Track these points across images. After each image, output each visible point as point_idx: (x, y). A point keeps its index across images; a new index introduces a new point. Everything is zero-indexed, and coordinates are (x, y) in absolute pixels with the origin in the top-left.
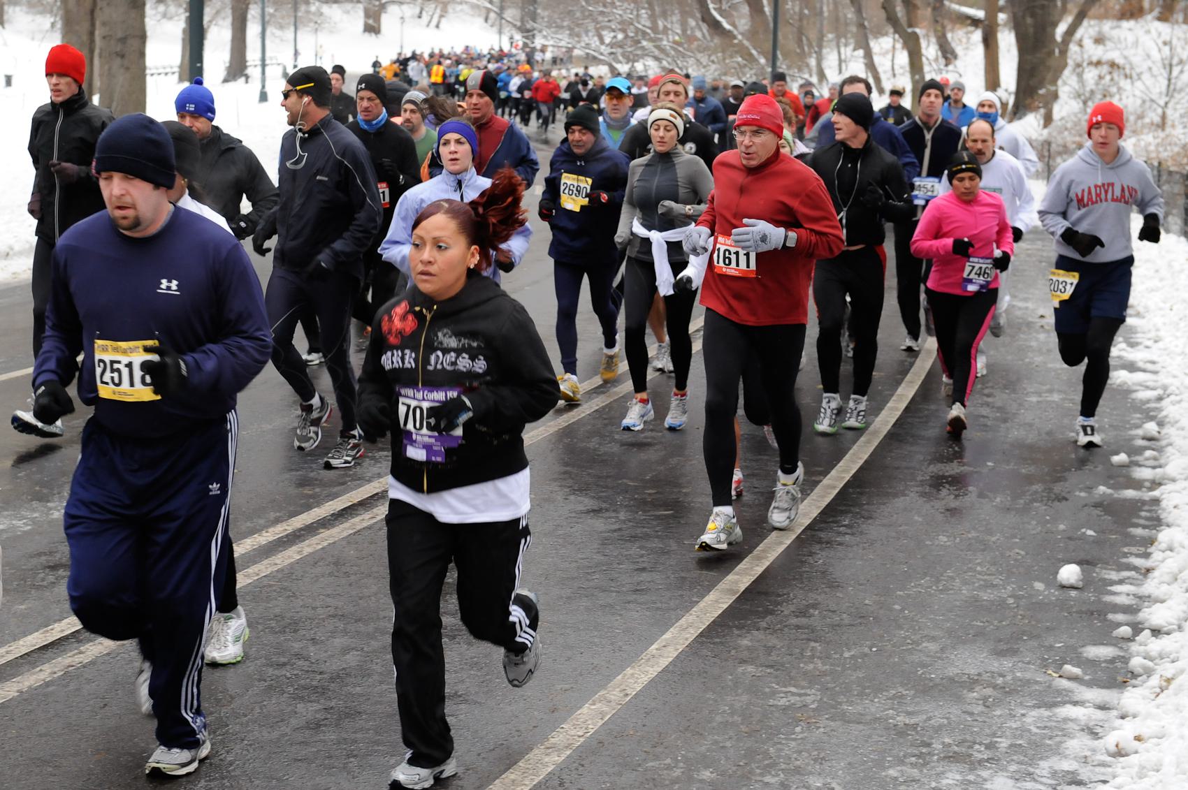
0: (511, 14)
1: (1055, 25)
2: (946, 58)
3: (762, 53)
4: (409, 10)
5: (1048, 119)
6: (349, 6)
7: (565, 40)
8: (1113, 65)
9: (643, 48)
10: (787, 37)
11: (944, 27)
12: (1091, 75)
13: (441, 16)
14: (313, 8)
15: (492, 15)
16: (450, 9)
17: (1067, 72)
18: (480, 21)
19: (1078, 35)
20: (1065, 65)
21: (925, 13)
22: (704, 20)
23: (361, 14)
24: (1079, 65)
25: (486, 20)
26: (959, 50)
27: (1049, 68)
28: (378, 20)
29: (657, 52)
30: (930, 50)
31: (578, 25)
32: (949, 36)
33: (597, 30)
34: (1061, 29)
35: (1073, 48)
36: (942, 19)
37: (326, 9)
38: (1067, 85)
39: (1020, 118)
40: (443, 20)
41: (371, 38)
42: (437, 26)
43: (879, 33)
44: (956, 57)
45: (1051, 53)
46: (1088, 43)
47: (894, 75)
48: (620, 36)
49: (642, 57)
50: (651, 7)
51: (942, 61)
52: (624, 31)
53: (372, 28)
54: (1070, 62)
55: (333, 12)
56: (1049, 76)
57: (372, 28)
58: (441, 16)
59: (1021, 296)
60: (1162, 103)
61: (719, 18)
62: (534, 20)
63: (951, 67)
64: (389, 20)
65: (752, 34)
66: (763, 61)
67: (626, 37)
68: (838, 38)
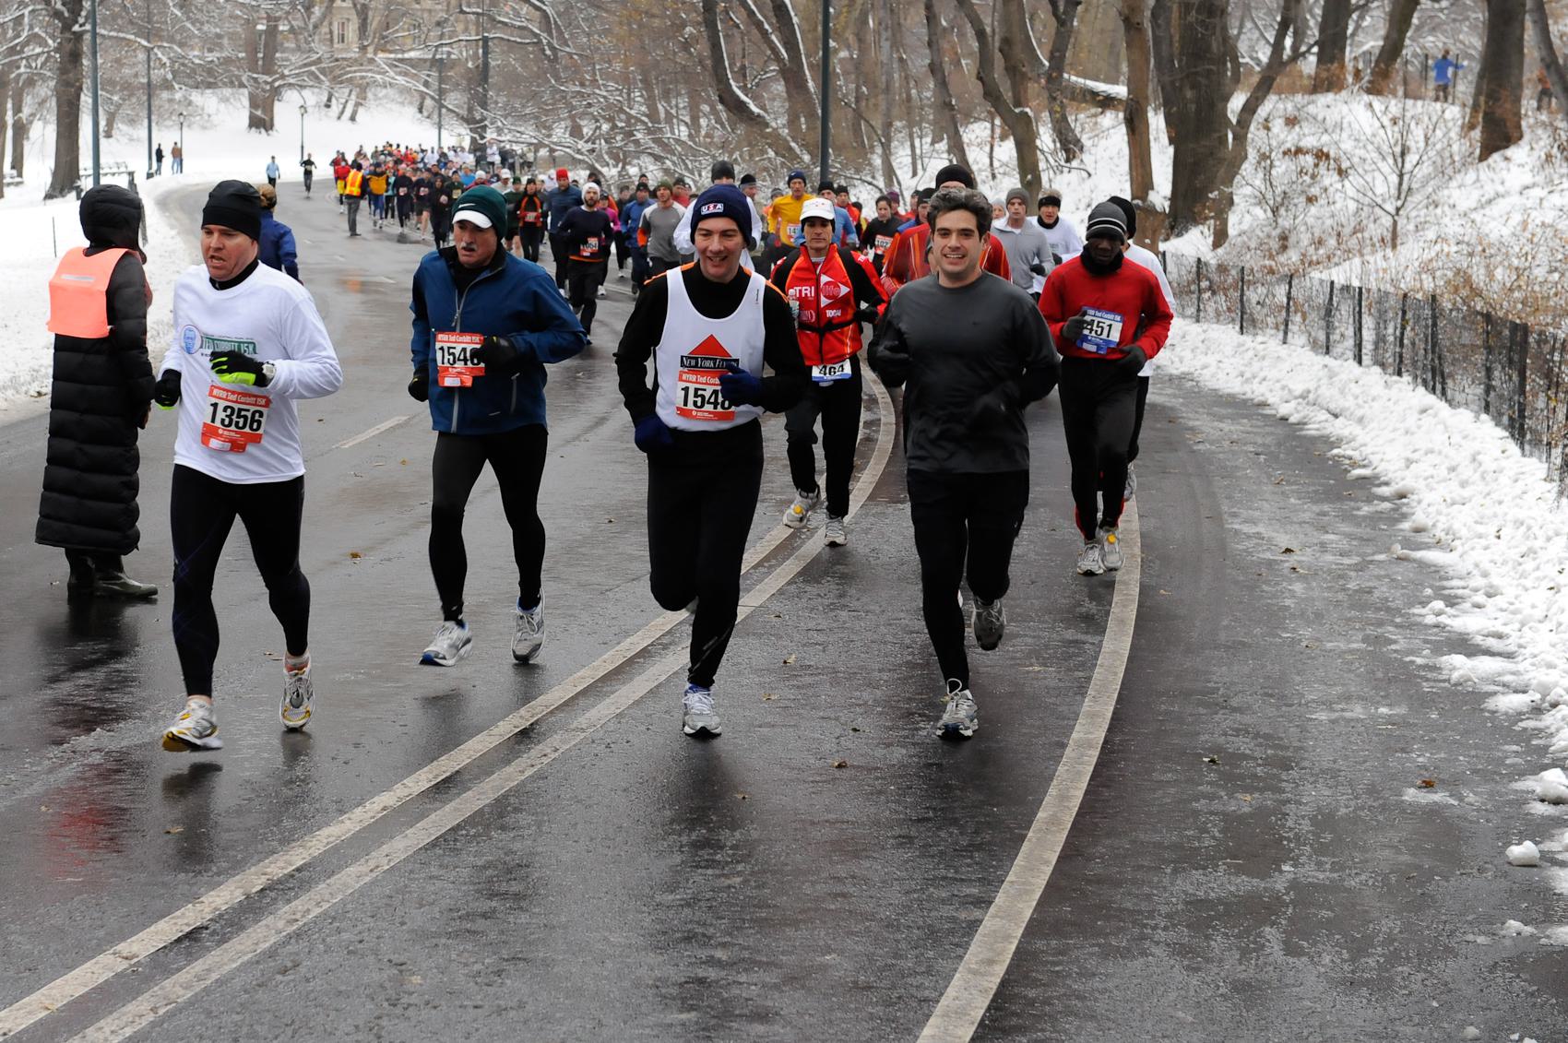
0: (455, 99)
1: (1227, 99)
2: (1067, 151)
3: (804, 146)
4: (312, 97)
5: (1220, 237)
6: (227, 92)
7: (529, 133)
8: (1321, 155)
9: (637, 142)
10: (840, 127)
11: (1062, 106)
12: (1282, 168)
13: (358, 105)
14: (178, 96)
15: (428, 102)
16: (370, 95)
17: (1247, 168)
18: (411, 111)
19: (1263, 111)
20: (1246, 157)
21: (1034, 88)
22: (722, 101)
23: (246, 102)
24: (1264, 157)
25: (420, 111)
26: (1084, 139)
27: (1221, 161)
28: (269, 110)
29: (657, 150)
30: (1046, 139)
31: (547, 113)
32: (1071, 119)
33: (572, 118)
34: (1237, 102)
35: (1255, 133)
36: (1062, 98)
37: (196, 97)
38: (1247, 186)
39: (1179, 235)
40: (361, 110)
41: (259, 137)
42: (353, 119)
43: (969, 117)
44: (1081, 149)
45: (1224, 140)
46: (1278, 126)
47: (994, 177)
48: (605, 127)
49: (638, 154)
50: (647, 85)
51: (1062, 155)
52: (610, 120)
53: (261, 122)
54: (1252, 155)
55: (206, 101)
56: (1222, 172)
57: (261, 122)
58: (358, 105)
59: (1244, 513)
60: (1391, 209)
61: (743, 97)
62: (484, 105)
63: (1075, 163)
64: (285, 110)
65: (793, 122)
66: (807, 158)
67: (614, 127)
68: (910, 126)
